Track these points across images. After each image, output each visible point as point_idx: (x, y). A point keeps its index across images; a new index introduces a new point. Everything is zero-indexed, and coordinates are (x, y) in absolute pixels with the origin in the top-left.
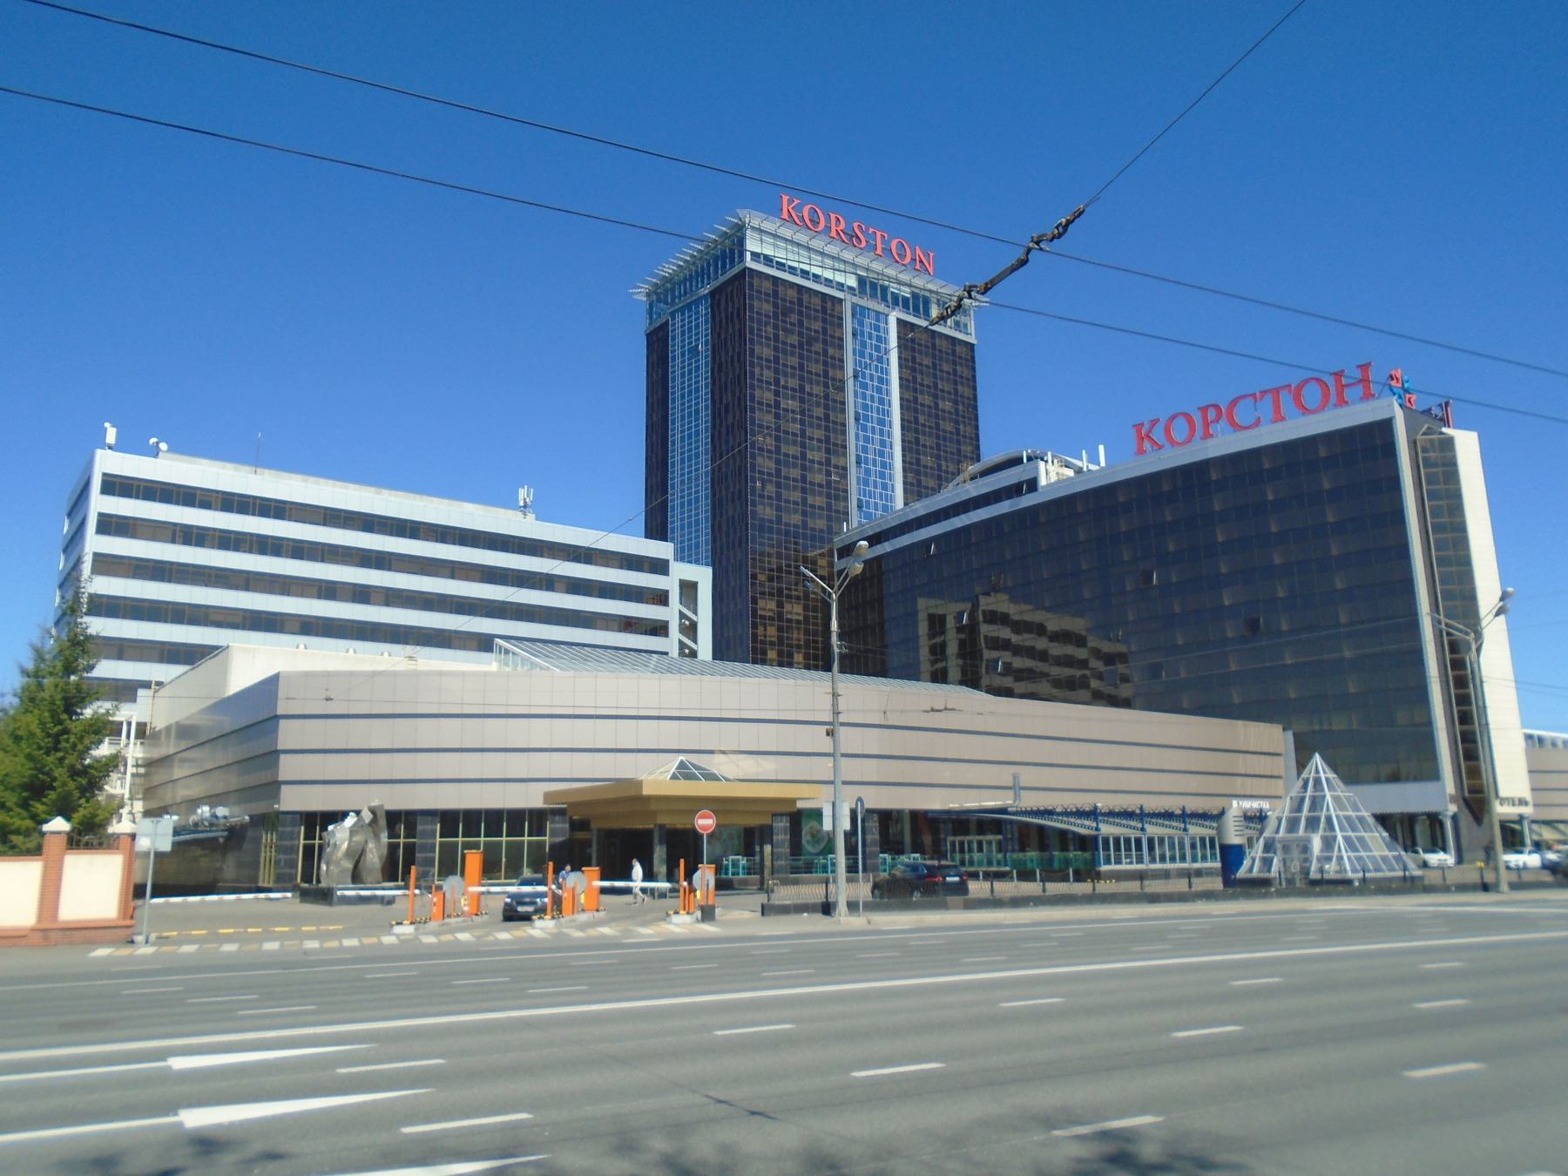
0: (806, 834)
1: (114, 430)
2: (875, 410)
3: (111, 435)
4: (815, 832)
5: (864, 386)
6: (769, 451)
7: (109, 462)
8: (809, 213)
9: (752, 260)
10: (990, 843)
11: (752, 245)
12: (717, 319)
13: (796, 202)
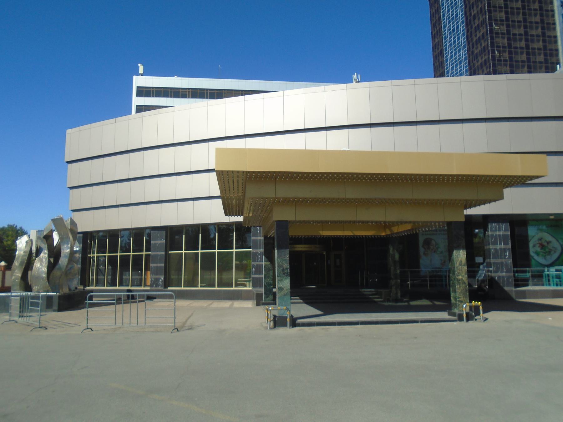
0: (534, 246)
1: (143, 66)
3: (141, 69)
4: (545, 244)
6: (503, 34)
7: (139, 81)
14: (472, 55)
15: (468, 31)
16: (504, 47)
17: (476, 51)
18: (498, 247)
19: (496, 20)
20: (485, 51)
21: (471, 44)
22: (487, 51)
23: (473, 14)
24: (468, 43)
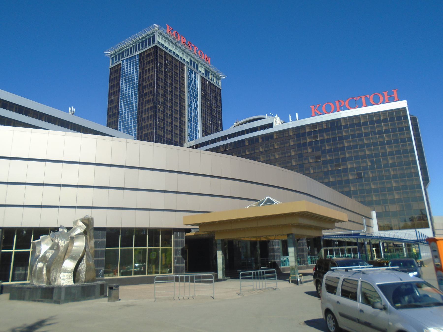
2: (194, 104)
5: (191, 95)
11: (158, 39)
12: (142, 64)
13: (172, 29)
14: (141, 117)
15: (139, 101)
16: (162, 119)
17: (144, 116)
19: (159, 102)
20: (151, 118)
21: (141, 110)
22: (152, 119)
23: (144, 92)
24: (139, 109)
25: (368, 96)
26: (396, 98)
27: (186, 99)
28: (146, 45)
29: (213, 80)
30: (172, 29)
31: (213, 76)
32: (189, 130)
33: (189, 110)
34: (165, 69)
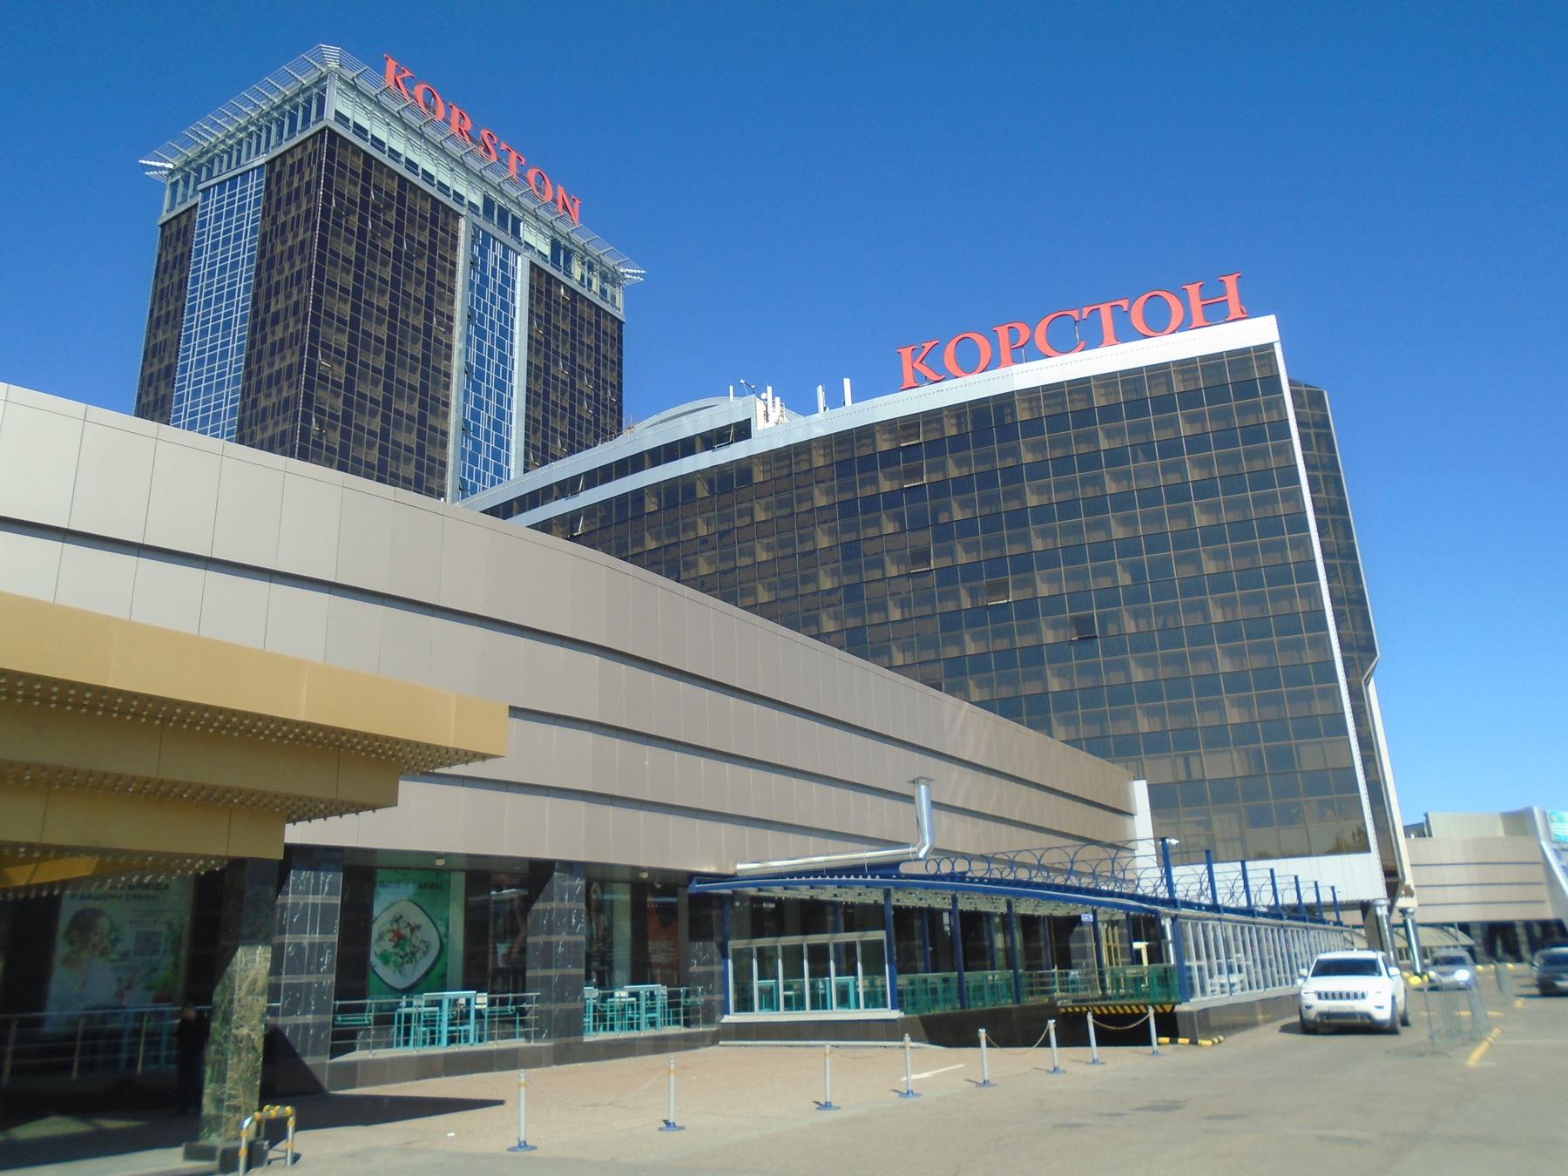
0: (381, 938)
2: (493, 368)
4: (406, 932)
5: (481, 333)
6: (336, 384)
8: (424, 95)
9: (336, 120)
10: (766, 958)
11: (338, 103)
12: (274, 199)
14: (252, 409)
15: (252, 345)
17: (263, 403)
18: (306, 939)
19: (326, 346)
20: (286, 409)
21: (254, 380)
22: (290, 413)
23: (273, 310)
24: (248, 376)
25: (1124, 303)
26: (1234, 307)
27: (458, 345)
28: (292, 129)
29: (586, 283)
30: (408, 73)
31: (591, 268)
32: (464, 466)
33: (468, 386)
34: (363, 220)
